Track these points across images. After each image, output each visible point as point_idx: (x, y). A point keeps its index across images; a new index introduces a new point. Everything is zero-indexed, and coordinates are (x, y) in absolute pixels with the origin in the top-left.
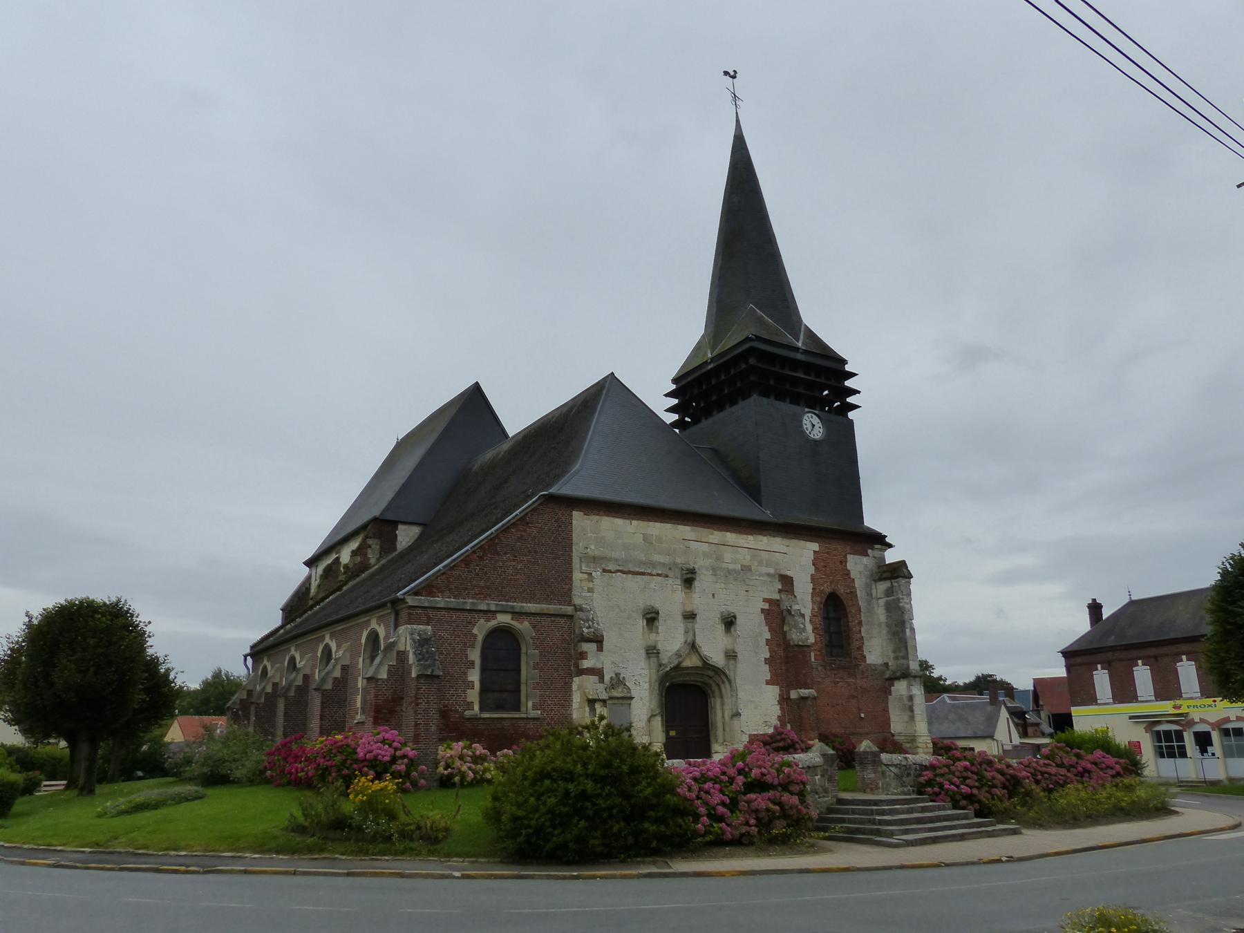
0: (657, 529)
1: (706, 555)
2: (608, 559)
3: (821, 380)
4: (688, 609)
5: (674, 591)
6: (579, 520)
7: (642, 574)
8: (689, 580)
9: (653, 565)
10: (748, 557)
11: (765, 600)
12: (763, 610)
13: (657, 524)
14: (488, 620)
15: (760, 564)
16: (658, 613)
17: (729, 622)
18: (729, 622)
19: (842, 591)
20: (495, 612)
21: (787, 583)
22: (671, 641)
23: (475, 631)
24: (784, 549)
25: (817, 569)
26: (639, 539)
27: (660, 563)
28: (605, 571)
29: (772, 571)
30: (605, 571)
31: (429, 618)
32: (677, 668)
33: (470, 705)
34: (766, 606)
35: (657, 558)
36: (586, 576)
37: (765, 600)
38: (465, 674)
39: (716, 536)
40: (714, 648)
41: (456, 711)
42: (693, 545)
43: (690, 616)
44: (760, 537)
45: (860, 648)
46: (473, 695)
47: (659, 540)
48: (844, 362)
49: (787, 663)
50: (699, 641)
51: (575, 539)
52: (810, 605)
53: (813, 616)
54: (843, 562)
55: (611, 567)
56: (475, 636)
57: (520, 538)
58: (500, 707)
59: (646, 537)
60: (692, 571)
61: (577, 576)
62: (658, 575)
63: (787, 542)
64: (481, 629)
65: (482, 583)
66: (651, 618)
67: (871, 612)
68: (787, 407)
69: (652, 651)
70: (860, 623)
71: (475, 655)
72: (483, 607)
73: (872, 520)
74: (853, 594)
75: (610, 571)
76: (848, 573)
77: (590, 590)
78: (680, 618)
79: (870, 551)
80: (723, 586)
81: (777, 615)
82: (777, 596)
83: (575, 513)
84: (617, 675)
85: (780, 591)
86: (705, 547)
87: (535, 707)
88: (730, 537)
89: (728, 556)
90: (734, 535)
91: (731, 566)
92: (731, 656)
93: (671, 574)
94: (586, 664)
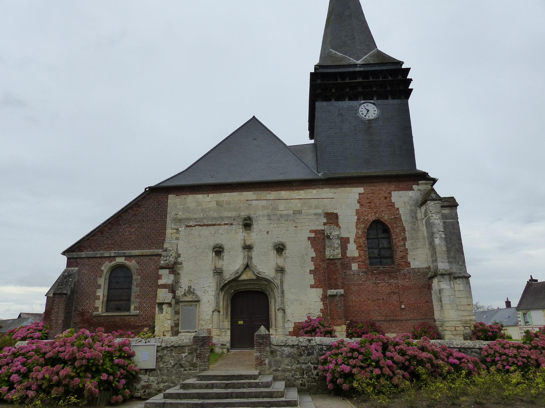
0: (226, 197)
1: (264, 207)
2: (190, 219)
3: (391, 82)
4: (248, 243)
5: (236, 233)
6: (173, 200)
7: (214, 225)
8: (247, 224)
9: (222, 218)
10: (299, 205)
11: (311, 231)
12: (309, 238)
13: (228, 194)
14: (110, 262)
15: (310, 207)
16: (223, 249)
17: (280, 249)
18: (280, 249)
19: (386, 218)
20: (115, 257)
21: (332, 218)
22: (232, 264)
23: (103, 268)
24: (332, 195)
25: (361, 205)
26: (214, 204)
27: (227, 217)
28: (187, 226)
29: (320, 211)
30: (187, 226)
31: (77, 263)
32: (235, 280)
33: (96, 309)
34: (313, 235)
35: (226, 214)
36: (175, 231)
37: (311, 231)
38: (95, 292)
39: (273, 195)
40: (265, 265)
41: (89, 312)
42: (254, 203)
43: (248, 248)
44: (310, 190)
45: (405, 257)
46: (99, 304)
47: (229, 203)
48: (401, 63)
49: (328, 272)
50: (255, 261)
51: (169, 211)
52: (354, 231)
53: (357, 237)
54: (388, 197)
55: (191, 223)
56: (102, 271)
57: (135, 215)
58: (118, 309)
59: (218, 203)
60: (249, 218)
61: (169, 231)
62: (225, 224)
63: (333, 190)
64: (106, 267)
65: (110, 242)
66: (219, 251)
67: (415, 230)
68: (346, 104)
69: (218, 272)
70: (405, 239)
71: (102, 281)
72: (107, 255)
73: (422, 164)
74: (398, 219)
75: (191, 226)
76: (393, 205)
77: (177, 239)
78: (240, 249)
79: (415, 187)
80: (276, 225)
81: (319, 240)
82: (322, 228)
83: (170, 196)
84: (190, 287)
85: (325, 224)
86: (264, 203)
87: (136, 309)
88: (284, 194)
89: (282, 206)
90: (288, 192)
91: (284, 213)
92: (281, 270)
93: (234, 223)
94: (160, 282)
